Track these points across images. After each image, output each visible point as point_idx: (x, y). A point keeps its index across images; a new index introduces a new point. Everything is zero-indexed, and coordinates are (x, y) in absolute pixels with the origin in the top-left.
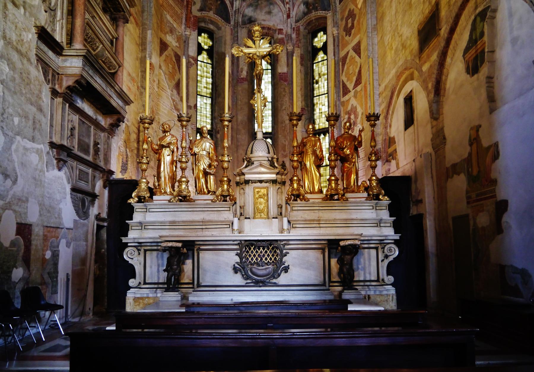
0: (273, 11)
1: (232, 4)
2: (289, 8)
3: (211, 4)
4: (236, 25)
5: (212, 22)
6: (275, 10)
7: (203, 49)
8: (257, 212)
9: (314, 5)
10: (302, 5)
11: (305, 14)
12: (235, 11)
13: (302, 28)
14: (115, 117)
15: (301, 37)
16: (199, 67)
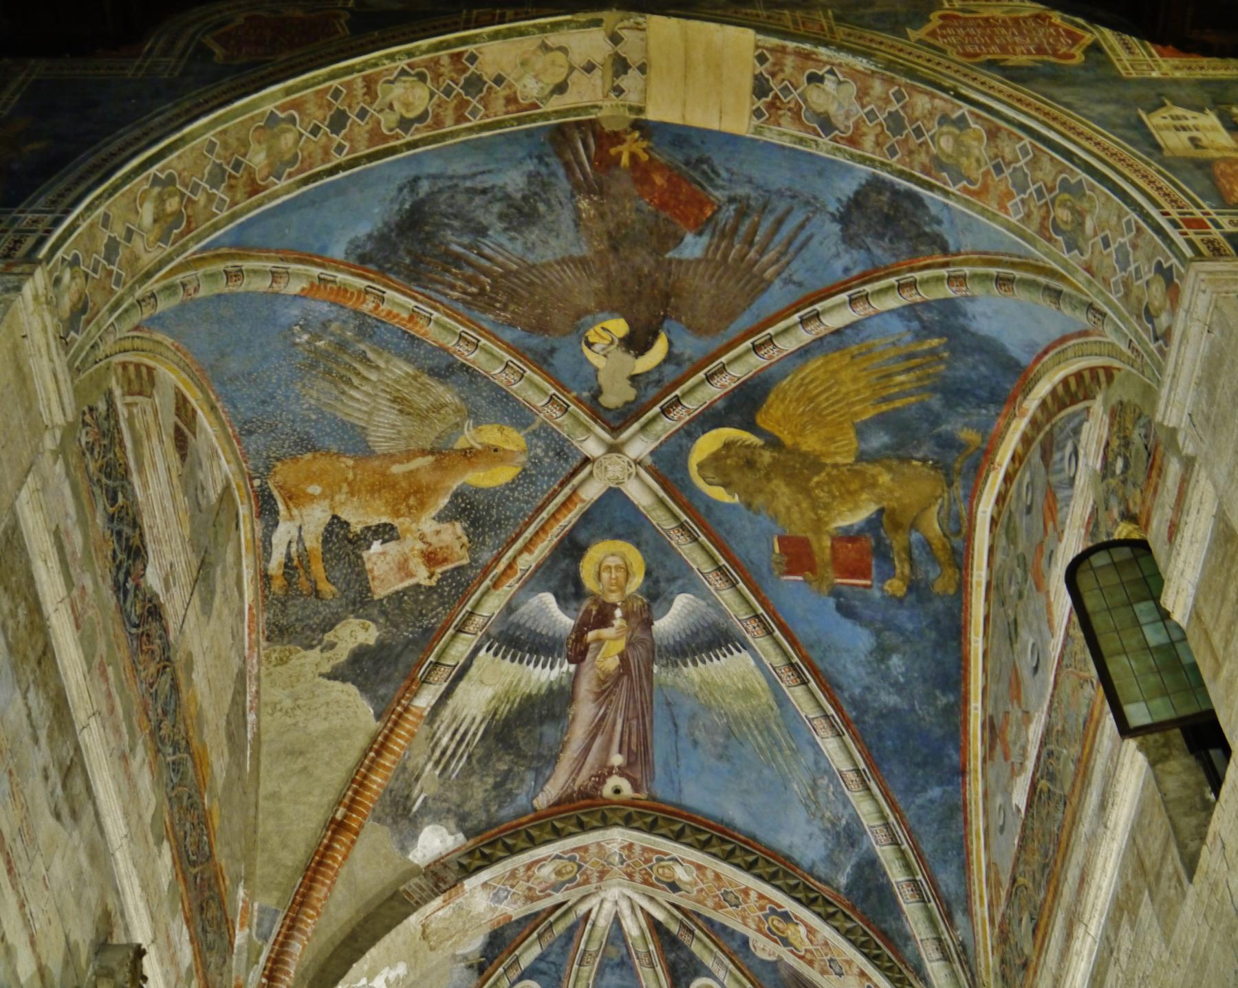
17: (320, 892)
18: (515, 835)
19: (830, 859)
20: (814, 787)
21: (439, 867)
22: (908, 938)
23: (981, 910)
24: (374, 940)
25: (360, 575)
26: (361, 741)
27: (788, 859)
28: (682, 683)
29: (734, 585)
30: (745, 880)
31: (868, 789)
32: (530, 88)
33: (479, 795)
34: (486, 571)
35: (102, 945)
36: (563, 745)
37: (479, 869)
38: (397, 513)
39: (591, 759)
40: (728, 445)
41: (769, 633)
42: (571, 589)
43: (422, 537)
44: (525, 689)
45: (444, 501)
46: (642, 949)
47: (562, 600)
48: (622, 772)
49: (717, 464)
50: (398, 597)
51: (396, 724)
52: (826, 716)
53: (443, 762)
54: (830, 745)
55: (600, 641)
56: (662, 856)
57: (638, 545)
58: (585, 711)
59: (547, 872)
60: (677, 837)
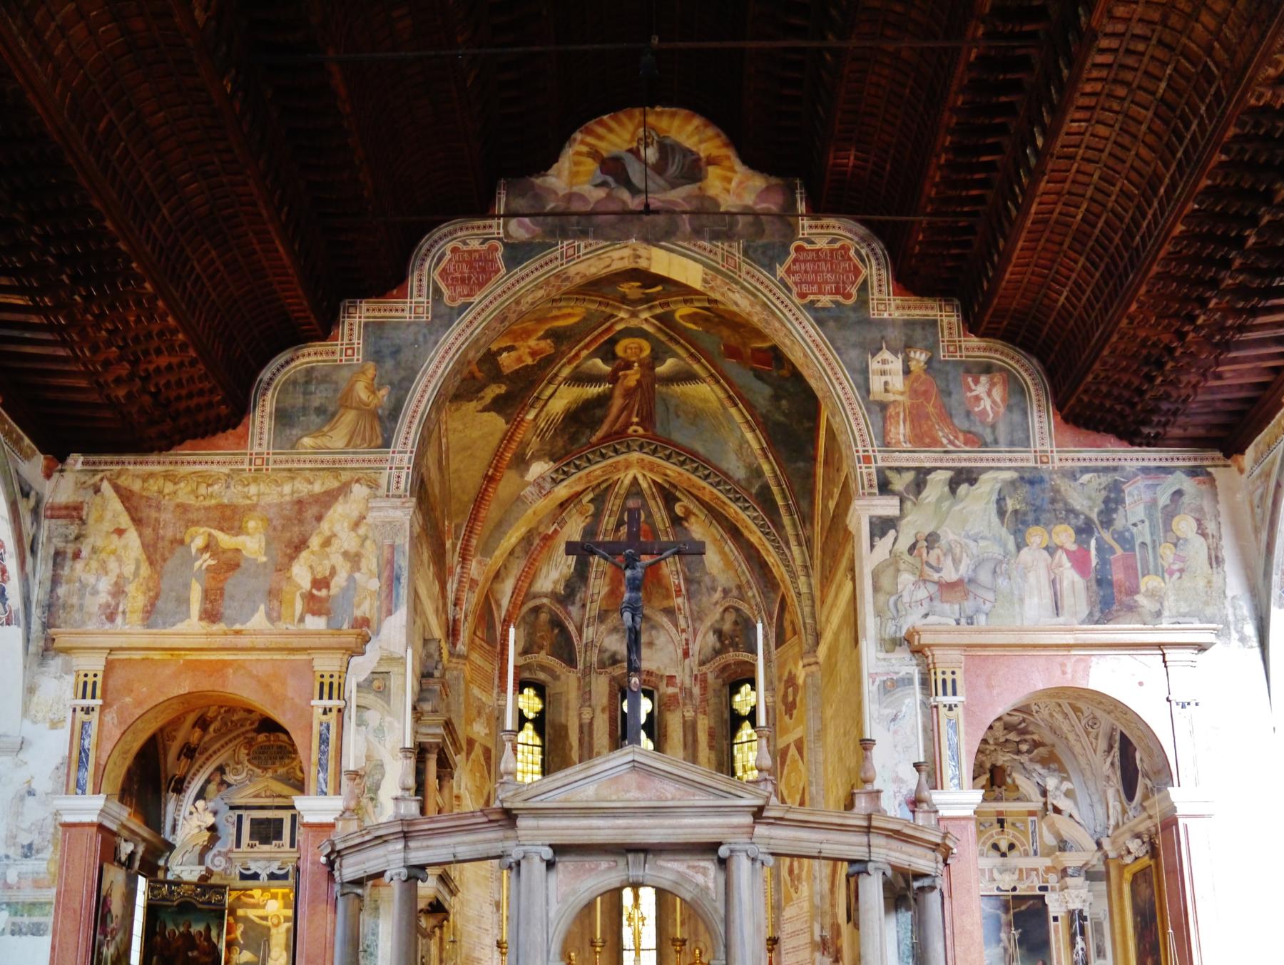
0: (657, 642)
1: (580, 631)
2: (687, 640)
3: (542, 637)
4: (588, 670)
5: (543, 668)
6: (661, 639)
7: (527, 720)
9: (732, 638)
10: (711, 633)
11: (717, 653)
12: (586, 645)
13: (710, 677)
14: (441, 916)
15: (710, 694)
16: (520, 756)
17: (483, 514)
18: (579, 458)
19: (748, 480)
20: (741, 447)
21: (540, 480)
22: (783, 527)
23: (818, 528)
24: (510, 526)
25: (497, 367)
26: (499, 435)
27: (726, 474)
28: (670, 391)
29: (699, 361)
30: (704, 484)
31: (767, 458)
32: (593, 270)
33: (560, 443)
34: (563, 354)
36: (605, 416)
37: (562, 480)
38: (516, 341)
39: (621, 420)
40: (695, 314)
41: (718, 382)
42: (610, 356)
43: (529, 347)
44: (585, 397)
45: (541, 333)
46: (649, 492)
47: (605, 361)
48: (637, 424)
49: (692, 318)
50: (517, 372)
51: (517, 427)
52: (747, 422)
53: (542, 435)
54: (749, 436)
55: (626, 376)
56: (659, 466)
57: (647, 339)
58: (617, 402)
59: (599, 472)
60: (668, 458)
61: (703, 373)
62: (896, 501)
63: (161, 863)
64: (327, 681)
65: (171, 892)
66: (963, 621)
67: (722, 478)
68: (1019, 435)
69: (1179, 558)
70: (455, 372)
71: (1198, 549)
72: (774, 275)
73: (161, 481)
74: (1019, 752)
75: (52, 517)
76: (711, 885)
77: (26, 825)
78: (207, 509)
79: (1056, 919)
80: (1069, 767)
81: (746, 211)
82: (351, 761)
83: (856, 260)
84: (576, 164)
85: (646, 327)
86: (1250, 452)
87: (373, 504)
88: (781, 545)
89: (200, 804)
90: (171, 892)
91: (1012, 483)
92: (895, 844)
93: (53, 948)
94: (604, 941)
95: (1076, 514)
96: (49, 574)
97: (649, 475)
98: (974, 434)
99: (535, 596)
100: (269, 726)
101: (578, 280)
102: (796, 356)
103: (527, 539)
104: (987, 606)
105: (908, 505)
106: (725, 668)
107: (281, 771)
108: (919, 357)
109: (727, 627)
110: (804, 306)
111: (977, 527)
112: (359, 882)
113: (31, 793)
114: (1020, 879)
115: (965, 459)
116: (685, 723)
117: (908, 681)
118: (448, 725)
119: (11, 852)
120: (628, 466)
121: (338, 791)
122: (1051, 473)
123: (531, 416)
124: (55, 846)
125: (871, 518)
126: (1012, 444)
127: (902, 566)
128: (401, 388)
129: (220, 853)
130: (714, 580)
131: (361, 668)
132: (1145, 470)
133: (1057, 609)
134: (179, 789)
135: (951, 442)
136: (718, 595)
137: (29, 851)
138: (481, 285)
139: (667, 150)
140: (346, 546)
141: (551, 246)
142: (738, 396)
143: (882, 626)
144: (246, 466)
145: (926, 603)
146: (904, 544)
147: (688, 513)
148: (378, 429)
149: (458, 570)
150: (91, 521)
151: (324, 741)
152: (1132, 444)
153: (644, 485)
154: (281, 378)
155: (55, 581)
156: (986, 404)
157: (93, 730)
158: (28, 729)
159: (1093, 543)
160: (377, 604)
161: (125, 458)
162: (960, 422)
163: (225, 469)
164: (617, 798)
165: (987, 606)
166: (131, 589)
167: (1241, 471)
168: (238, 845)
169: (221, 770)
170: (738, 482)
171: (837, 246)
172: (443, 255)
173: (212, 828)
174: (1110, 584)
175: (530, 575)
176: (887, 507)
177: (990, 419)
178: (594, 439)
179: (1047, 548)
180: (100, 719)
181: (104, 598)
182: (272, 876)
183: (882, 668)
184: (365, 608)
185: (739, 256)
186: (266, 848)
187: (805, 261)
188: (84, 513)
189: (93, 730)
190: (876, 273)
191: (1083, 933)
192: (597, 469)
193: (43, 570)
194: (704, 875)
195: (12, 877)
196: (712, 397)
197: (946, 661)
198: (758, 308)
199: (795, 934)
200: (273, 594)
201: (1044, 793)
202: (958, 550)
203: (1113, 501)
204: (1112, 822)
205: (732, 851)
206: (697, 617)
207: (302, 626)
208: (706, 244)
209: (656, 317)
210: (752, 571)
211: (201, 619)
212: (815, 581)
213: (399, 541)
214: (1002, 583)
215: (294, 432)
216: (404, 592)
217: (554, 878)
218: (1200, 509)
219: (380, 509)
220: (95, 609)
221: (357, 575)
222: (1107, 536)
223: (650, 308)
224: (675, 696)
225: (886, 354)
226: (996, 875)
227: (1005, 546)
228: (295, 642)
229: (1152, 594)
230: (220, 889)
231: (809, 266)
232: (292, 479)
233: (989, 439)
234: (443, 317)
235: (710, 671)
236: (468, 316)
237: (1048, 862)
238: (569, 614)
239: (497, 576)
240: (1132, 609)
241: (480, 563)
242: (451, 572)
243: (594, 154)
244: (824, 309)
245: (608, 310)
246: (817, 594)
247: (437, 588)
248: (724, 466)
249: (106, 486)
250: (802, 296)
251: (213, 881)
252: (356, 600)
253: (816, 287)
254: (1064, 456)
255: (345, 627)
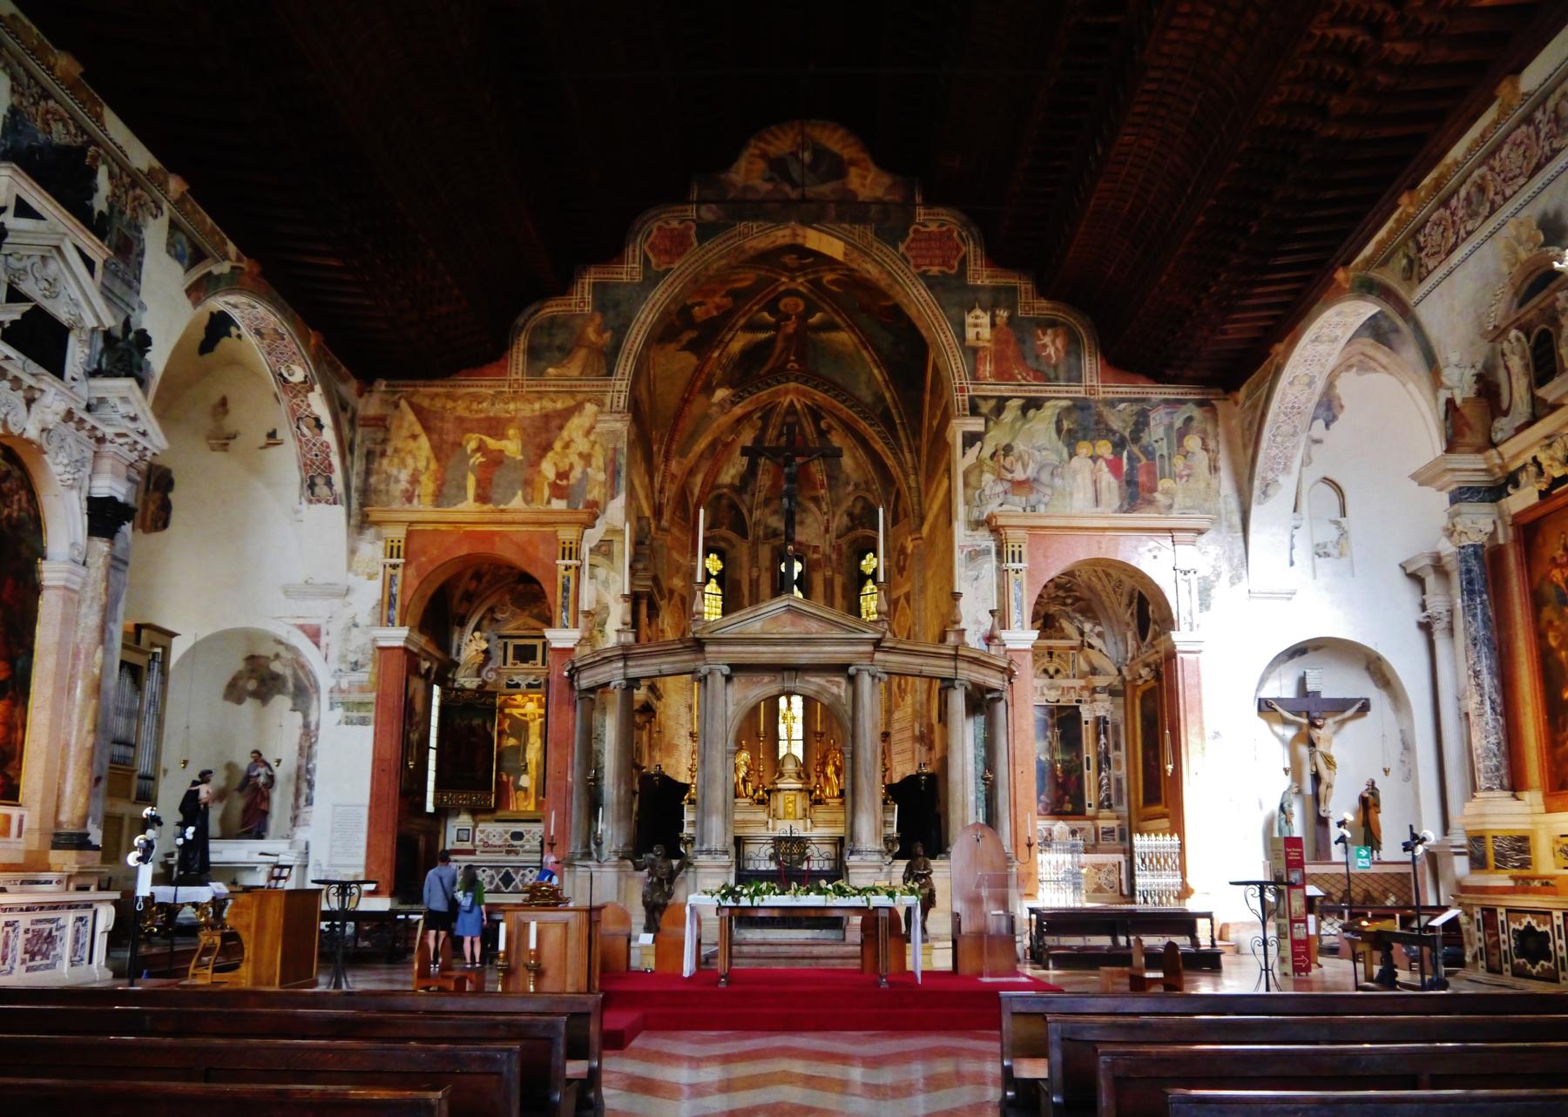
5: (724, 539)
6: (809, 520)
7: (712, 576)
8: (786, 815)
11: (849, 529)
13: (844, 547)
23: (925, 440)
26: (691, 369)
27: (858, 399)
29: (840, 316)
30: (842, 406)
32: (763, 245)
35: (639, 519)
41: (854, 331)
45: (723, 293)
49: (833, 282)
52: (874, 361)
53: (724, 368)
54: (876, 371)
58: (780, 345)
60: (816, 387)
61: (843, 325)
62: (982, 421)
63: (450, 676)
64: (567, 546)
65: (457, 696)
66: (1028, 509)
67: (855, 402)
68: (1074, 374)
69: (1187, 467)
70: (661, 320)
71: (1201, 460)
72: (897, 250)
73: (444, 400)
74: (1065, 604)
75: (363, 426)
76: (843, 694)
77: (352, 648)
78: (479, 420)
79: (1086, 722)
80: (1100, 616)
81: (878, 201)
82: (586, 603)
83: (958, 240)
84: (751, 163)
85: (801, 289)
86: (1243, 391)
87: (601, 417)
88: (896, 450)
89: (477, 634)
90: (457, 696)
91: (1068, 410)
92: (975, 667)
93: (375, 734)
94: (765, 732)
95: (1114, 432)
96: (364, 467)
97: (802, 399)
98: (1042, 372)
99: (719, 487)
100: (527, 579)
101: (751, 253)
102: (912, 312)
103: (713, 445)
104: (1046, 499)
105: (991, 424)
106: (855, 541)
107: (535, 611)
108: (1003, 314)
109: (857, 511)
110: (920, 274)
111: (1041, 441)
112: (592, 690)
113: (356, 625)
114: (1062, 694)
115: (1034, 391)
116: (825, 580)
117: (988, 552)
118: (655, 579)
119: (343, 667)
120: (787, 392)
121: (576, 626)
122: (1097, 402)
123: (716, 354)
124: (374, 662)
125: (964, 433)
126: (1069, 380)
127: (985, 468)
128: (620, 332)
129: (491, 670)
130: (848, 477)
131: (593, 536)
132: (1166, 402)
133: (1097, 501)
134: (462, 624)
135: (1024, 378)
136: (850, 488)
137: (355, 666)
138: (679, 255)
139: (820, 153)
140: (581, 449)
141: (731, 226)
142: (868, 341)
143: (969, 513)
144: (506, 389)
145: (1002, 496)
146: (987, 452)
147: (830, 428)
148: (604, 362)
149: (662, 467)
150: (393, 429)
151: (566, 589)
152: (1158, 382)
153: (798, 406)
154: (532, 323)
155: (368, 473)
156: (1051, 350)
157: (399, 581)
158: (352, 579)
159: (1125, 454)
160: (603, 491)
161: (418, 382)
162: (1031, 362)
163: (491, 391)
164: (776, 631)
165: (1046, 499)
166: (424, 478)
167: (1236, 403)
168: (505, 664)
169: (491, 610)
170: (867, 405)
171: (944, 229)
172: (651, 232)
173: (486, 652)
174: (1136, 484)
175: (715, 472)
176: (976, 425)
177: (1054, 360)
178: (762, 372)
179: (1091, 457)
180: (404, 576)
181: (404, 485)
182: (529, 686)
183: (969, 541)
184: (595, 493)
185: (870, 235)
186: (525, 665)
187: (920, 240)
188: (388, 423)
189: (399, 581)
190: (971, 249)
191: (1105, 732)
192: (764, 394)
193: (358, 466)
194: (838, 688)
195: (344, 684)
196: (849, 342)
197: (1015, 537)
198: (884, 276)
199: (902, 730)
200: (528, 483)
201: (1082, 634)
202: (1026, 457)
203: (1141, 423)
204: (1130, 655)
205: (858, 670)
206: (835, 503)
207: (549, 507)
208: (846, 226)
209: (807, 281)
210: (875, 471)
211: (475, 501)
212: (922, 479)
213: (619, 445)
214: (1058, 482)
215: (543, 364)
216: (623, 483)
217: (730, 689)
218: (1205, 431)
219: (605, 421)
220: (397, 493)
221: (589, 470)
222: (1135, 449)
223: (805, 275)
224: (818, 561)
225: (978, 312)
226: (1046, 691)
227: (1060, 455)
228: (545, 518)
229: (1166, 493)
230: (493, 695)
231: (923, 244)
232: (540, 398)
233: (1052, 376)
234: (652, 279)
235: (844, 542)
236: (669, 279)
237: (1082, 682)
238: (743, 501)
239: (692, 472)
240: (1151, 502)
241: (678, 462)
242: (658, 469)
243: (764, 156)
244: (933, 276)
245: (774, 276)
246: (923, 488)
247: (647, 479)
248: (857, 393)
249: (403, 403)
250: (917, 266)
251: (488, 688)
252: (588, 487)
253: (928, 261)
254: (1107, 389)
255: (581, 507)
